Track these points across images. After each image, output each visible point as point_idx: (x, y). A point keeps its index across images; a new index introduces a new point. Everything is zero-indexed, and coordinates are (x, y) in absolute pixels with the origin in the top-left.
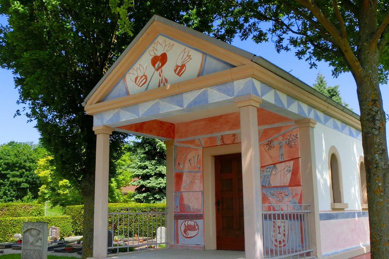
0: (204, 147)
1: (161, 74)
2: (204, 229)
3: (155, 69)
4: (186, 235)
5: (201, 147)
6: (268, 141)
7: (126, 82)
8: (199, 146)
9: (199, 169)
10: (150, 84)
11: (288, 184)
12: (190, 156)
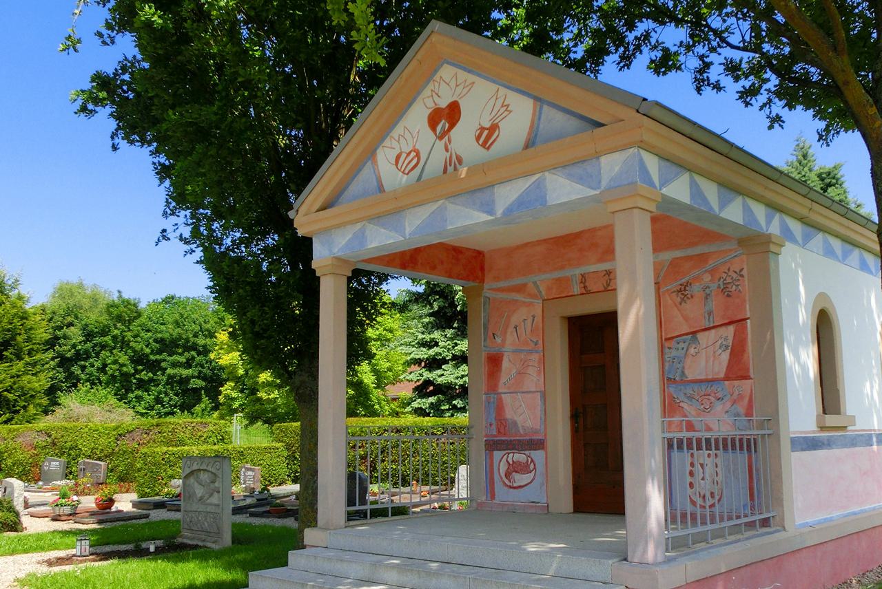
0: (546, 300)
1: (449, 147)
3: (436, 135)
6: (681, 285)
9: (536, 345)
10: (427, 167)
11: (722, 375)
12: (515, 319)
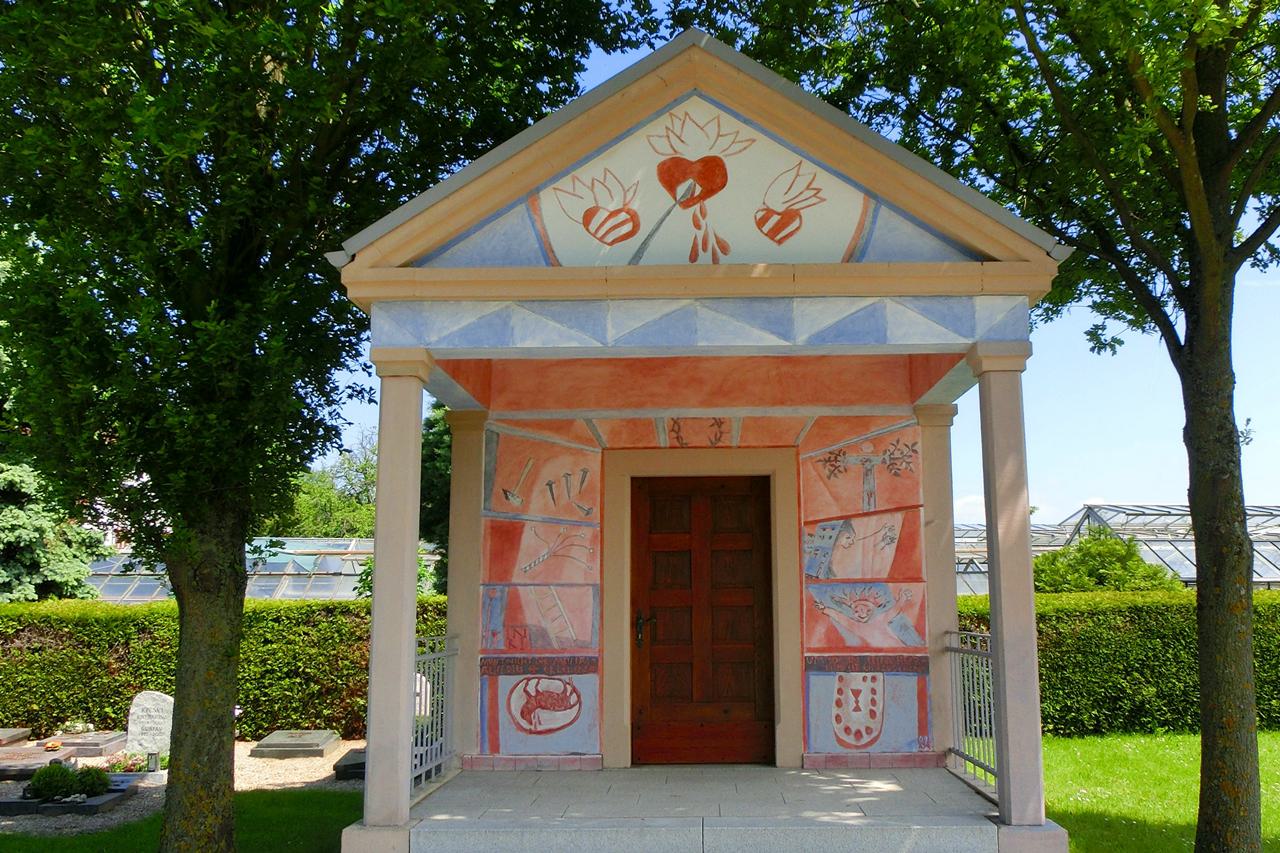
0: (608, 449)
1: (703, 222)
2: (601, 705)
3: (675, 199)
4: (531, 723)
5: (595, 447)
6: (830, 453)
7: (540, 216)
8: (589, 442)
9: (588, 514)
10: (653, 243)
11: (885, 575)
12: (549, 472)
